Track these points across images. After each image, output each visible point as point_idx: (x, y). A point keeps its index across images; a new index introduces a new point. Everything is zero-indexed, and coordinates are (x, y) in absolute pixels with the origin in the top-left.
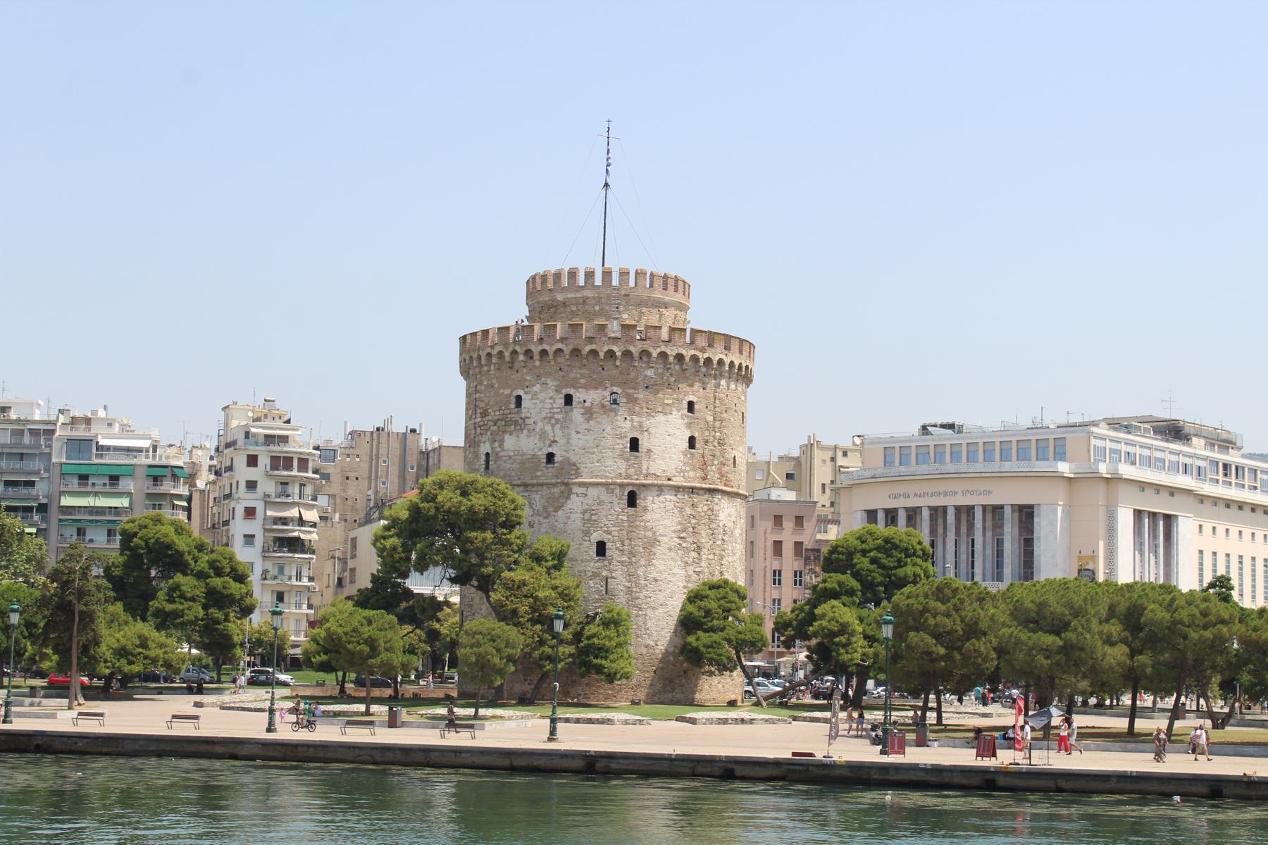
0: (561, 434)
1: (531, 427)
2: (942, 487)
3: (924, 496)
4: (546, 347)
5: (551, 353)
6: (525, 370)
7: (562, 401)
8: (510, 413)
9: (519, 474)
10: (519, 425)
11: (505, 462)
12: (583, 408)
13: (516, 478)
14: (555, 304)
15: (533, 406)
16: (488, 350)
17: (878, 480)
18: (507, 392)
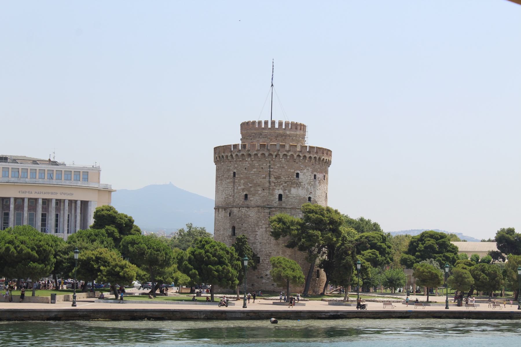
0: (313, 190)
1: (303, 186)
2: (50, 190)
3: (40, 193)
4: (312, 155)
5: (313, 158)
6: (300, 163)
7: (313, 177)
8: (294, 180)
9: (298, 204)
10: (298, 185)
11: (291, 199)
12: (319, 180)
13: (297, 206)
14: (285, 135)
15: (304, 178)
16: (285, 153)
17: (15, 184)
18: (292, 171)
